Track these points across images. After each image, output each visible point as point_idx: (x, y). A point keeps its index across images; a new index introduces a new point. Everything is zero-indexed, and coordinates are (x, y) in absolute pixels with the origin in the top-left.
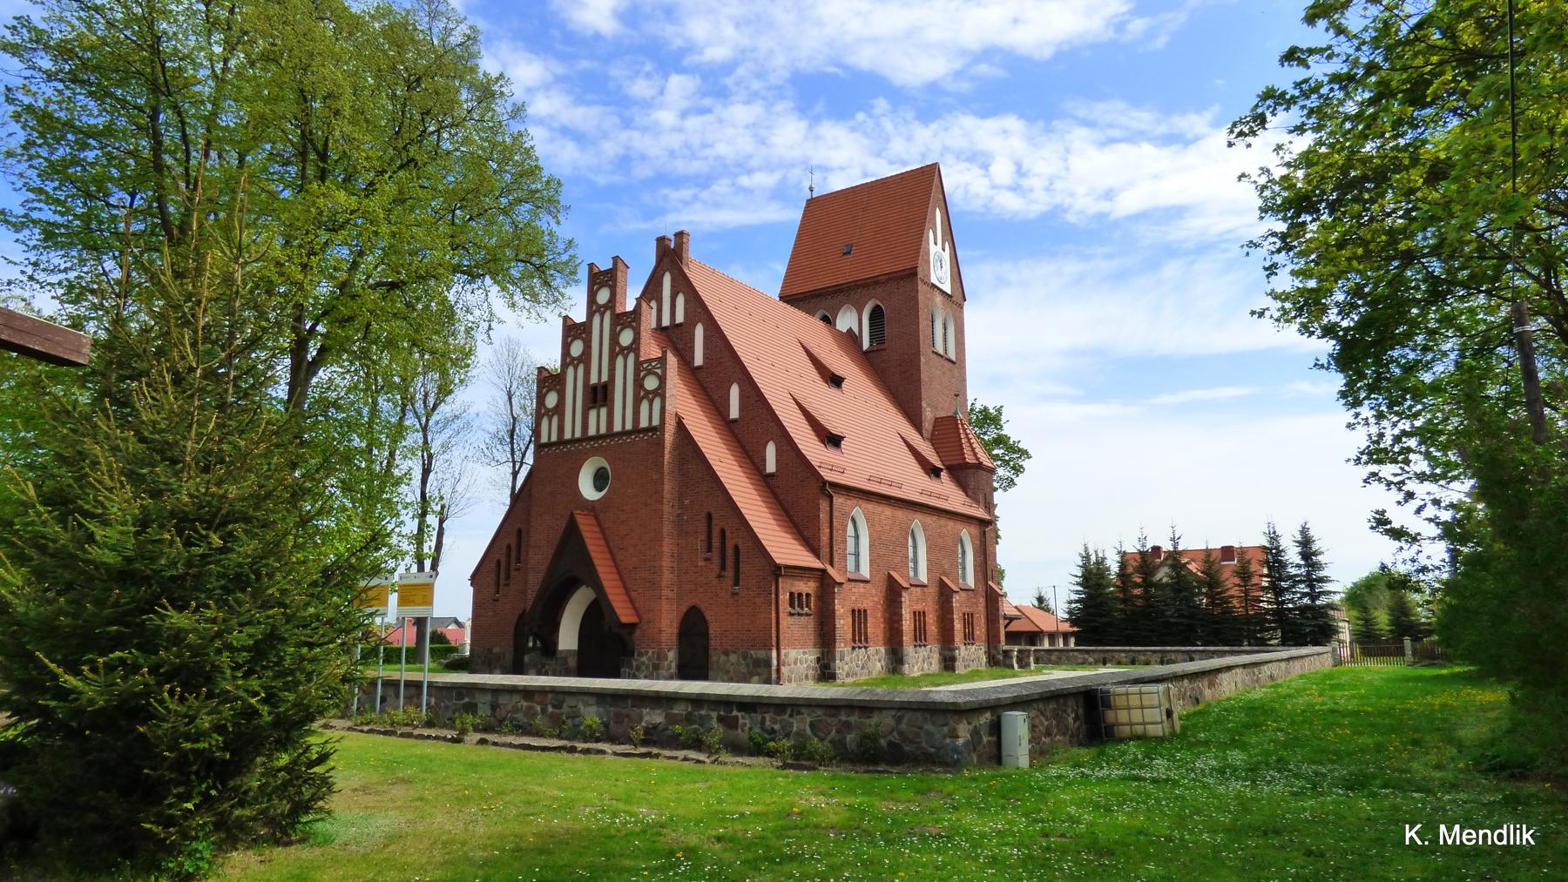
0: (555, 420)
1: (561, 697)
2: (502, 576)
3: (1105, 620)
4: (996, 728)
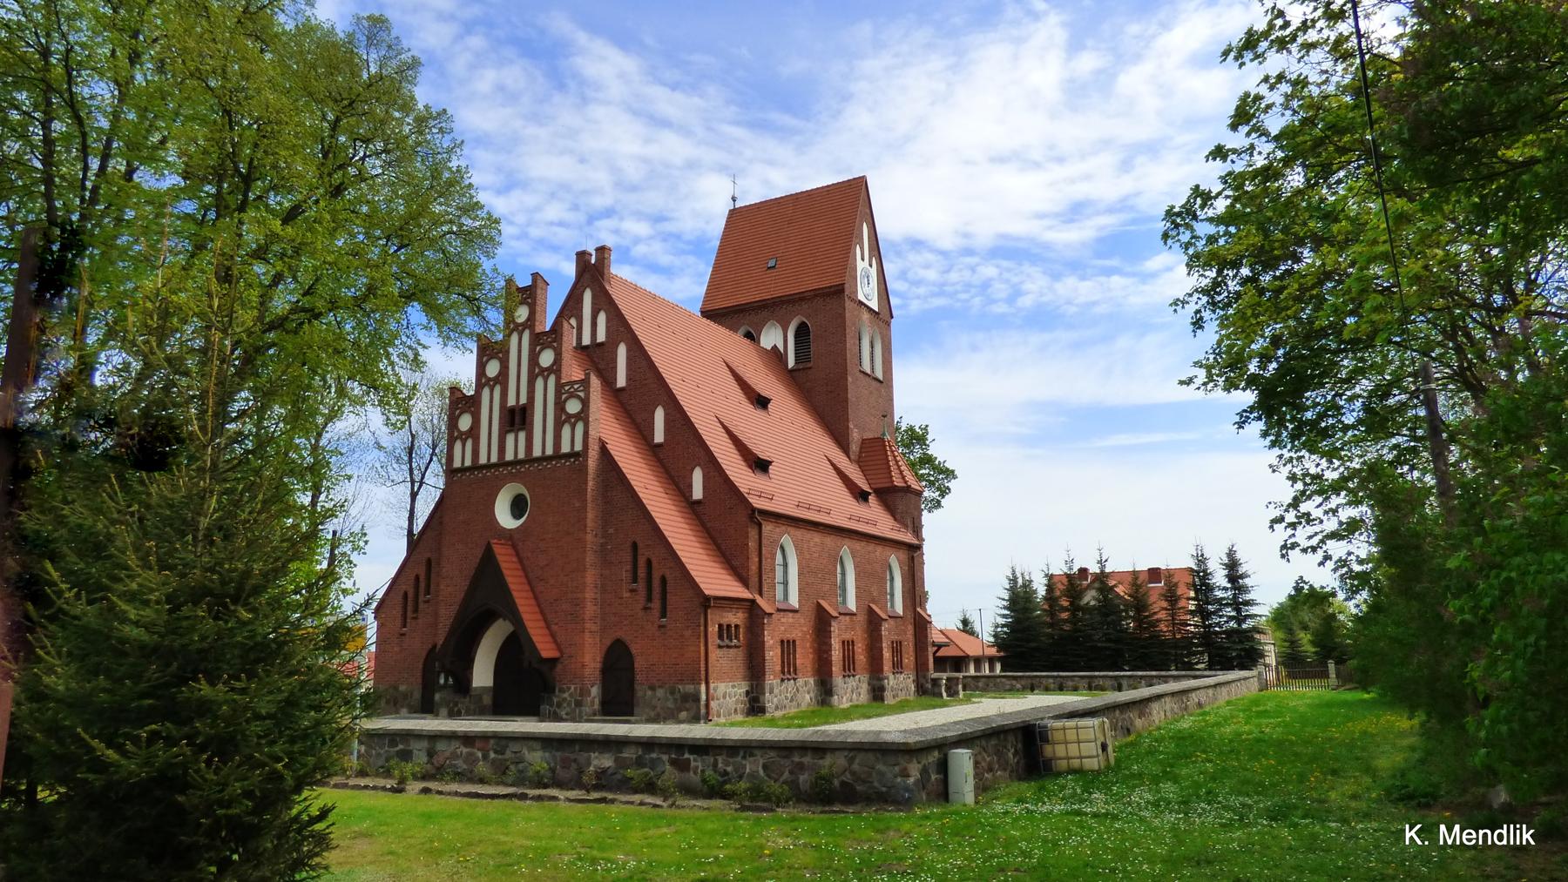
0: (469, 444)
1: (503, 742)
2: (410, 608)
3: (1033, 645)
4: (943, 766)
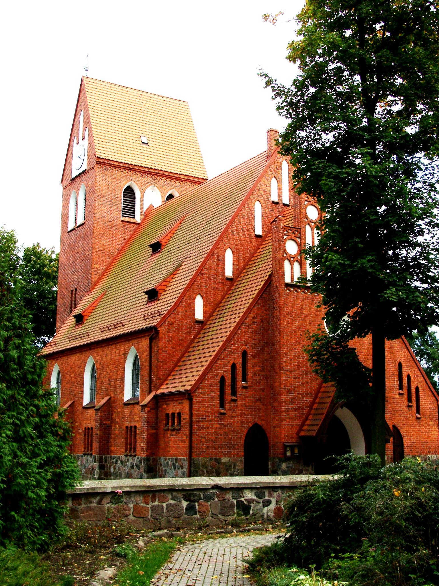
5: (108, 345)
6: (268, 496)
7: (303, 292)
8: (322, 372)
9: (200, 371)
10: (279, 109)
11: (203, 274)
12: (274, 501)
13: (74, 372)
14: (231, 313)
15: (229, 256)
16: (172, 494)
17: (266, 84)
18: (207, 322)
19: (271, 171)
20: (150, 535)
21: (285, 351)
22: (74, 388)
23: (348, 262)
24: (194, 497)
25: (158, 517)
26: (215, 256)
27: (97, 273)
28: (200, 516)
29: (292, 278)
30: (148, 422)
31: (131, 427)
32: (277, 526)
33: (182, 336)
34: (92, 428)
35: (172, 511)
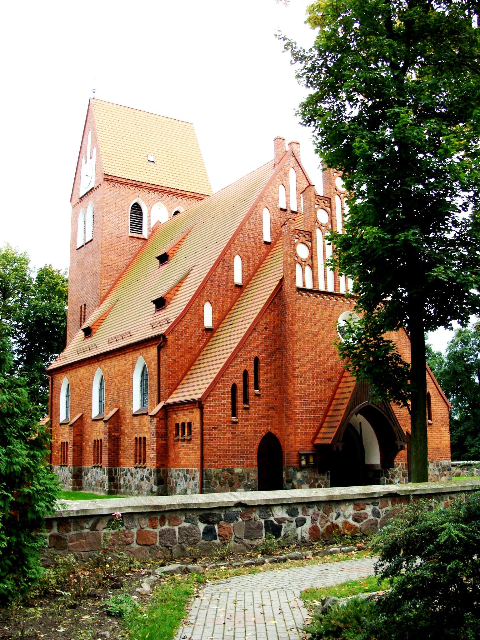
2: (240, 399)
5: (116, 356)
6: (302, 514)
7: (315, 296)
8: (355, 368)
9: (210, 378)
10: (298, 76)
11: (211, 281)
12: (309, 519)
13: (82, 384)
14: (242, 319)
15: (238, 263)
16: (185, 515)
17: (285, 48)
18: (216, 329)
19: (279, 178)
20: (159, 571)
21: (297, 357)
22: (83, 401)
23: (389, 236)
24: (213, 518)
25: (168, 544)
26: (223, 262)
27: (105, 288)
28: (221, 540)
29: (304, 283)
30: (157, 432)
31: (140, 438)
32: (319, 552)
33: (191, 344)
34: (101, 440)
35: (186, 535)
